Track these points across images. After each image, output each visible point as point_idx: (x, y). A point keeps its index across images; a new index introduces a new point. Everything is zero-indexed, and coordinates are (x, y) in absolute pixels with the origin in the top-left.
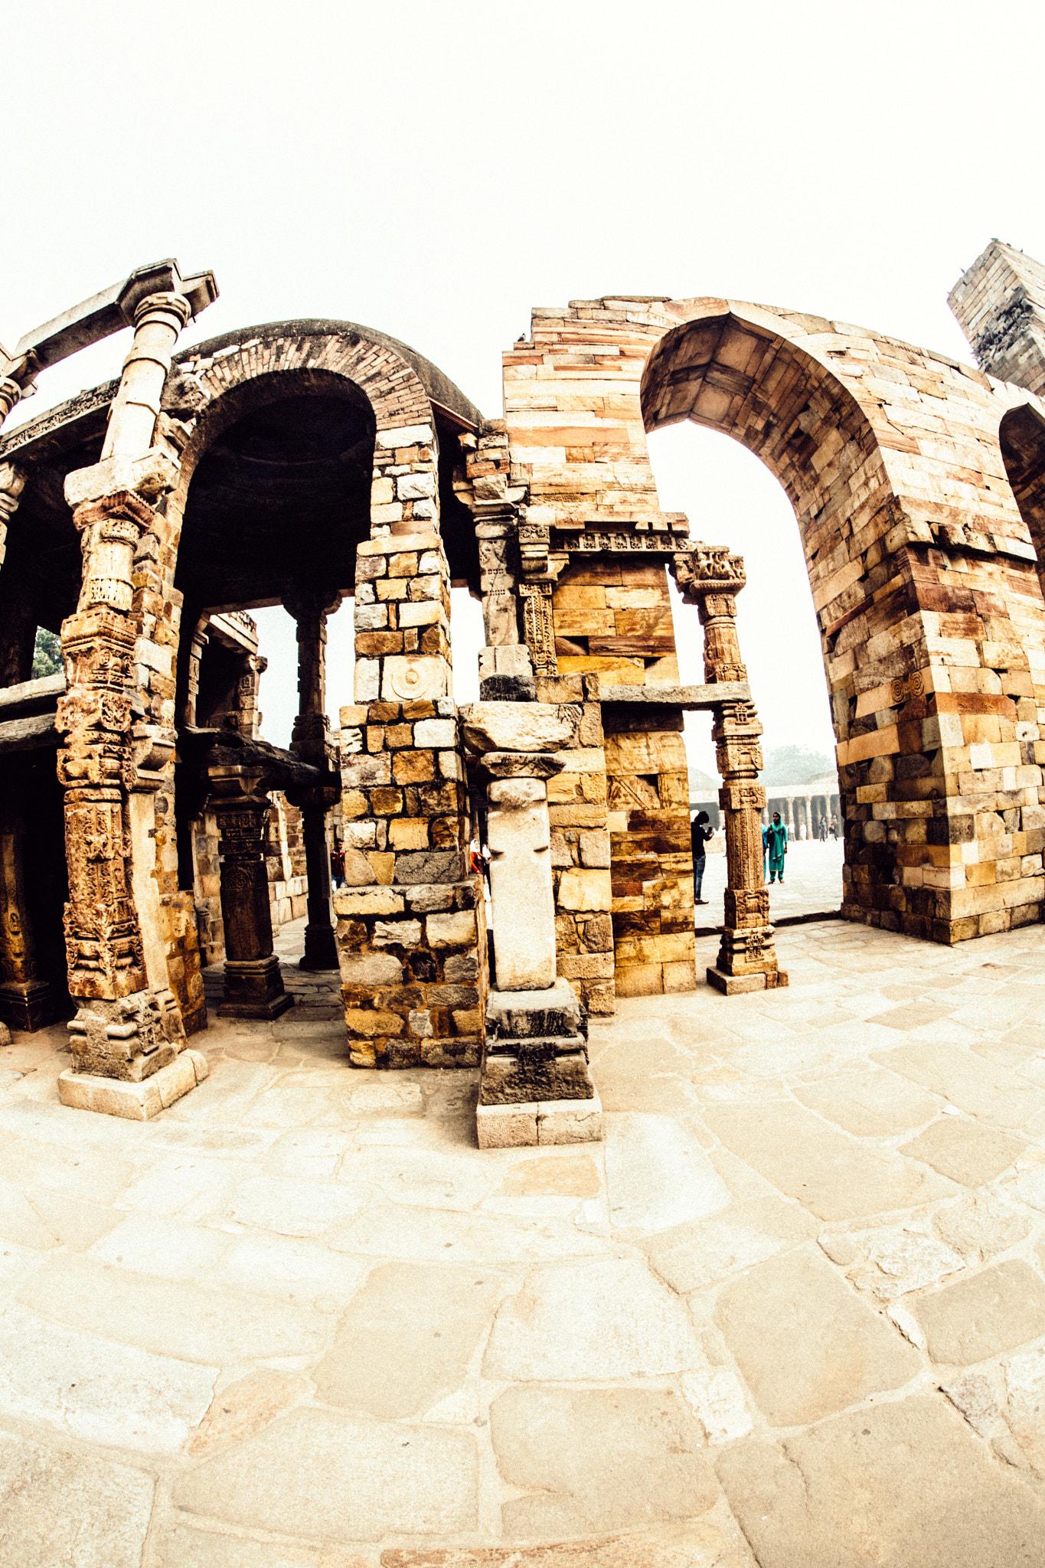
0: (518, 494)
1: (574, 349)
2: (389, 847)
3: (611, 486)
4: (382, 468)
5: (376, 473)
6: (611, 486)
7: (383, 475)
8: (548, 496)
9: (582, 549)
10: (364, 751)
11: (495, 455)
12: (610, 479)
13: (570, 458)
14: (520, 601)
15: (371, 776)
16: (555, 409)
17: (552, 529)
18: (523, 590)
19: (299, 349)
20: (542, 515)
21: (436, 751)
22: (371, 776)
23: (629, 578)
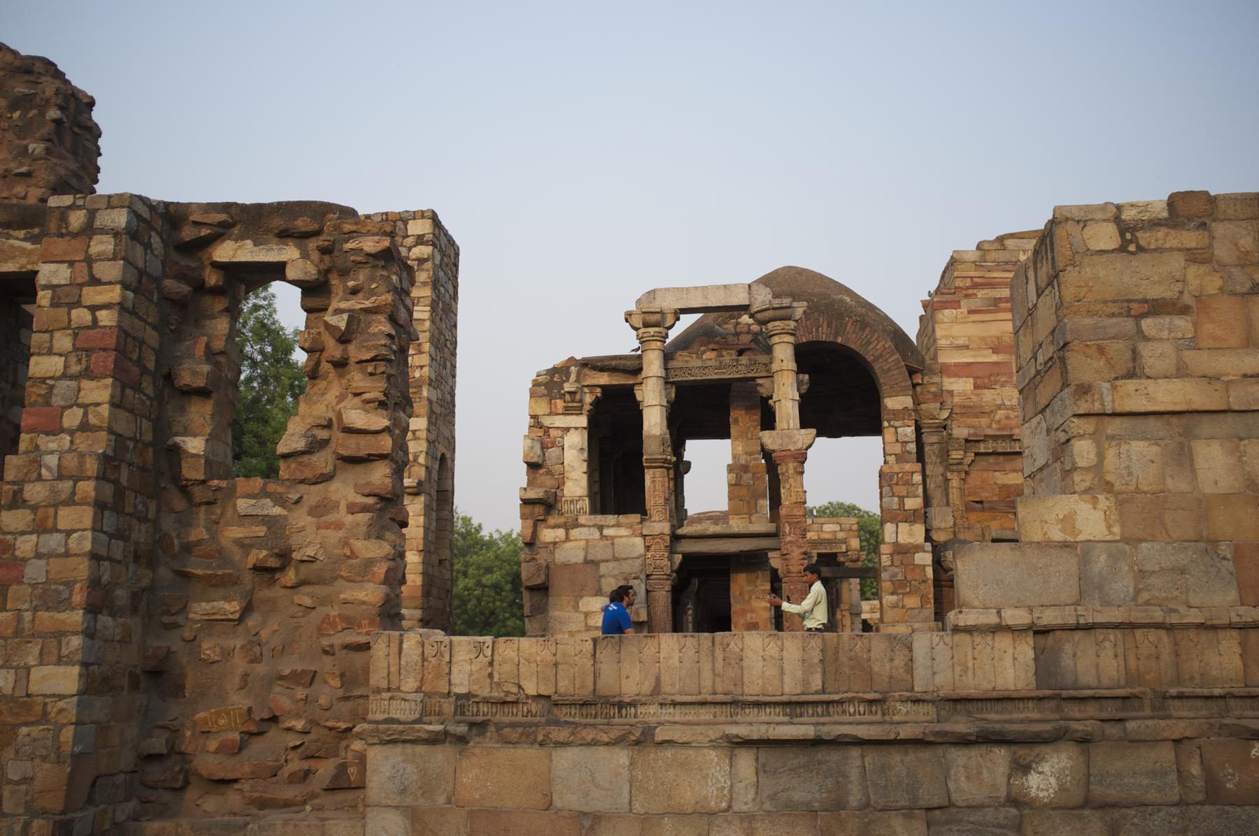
0: (945, 414)
1: (981, 293)
2: (903, 607)
3: (999, 407)
4: (889, 421)
5: (886, 424)
6: (999, 407)
7: (890, 426)
8: (962, 414)
9: (982, 450)
10: (892, 565)
11: (933, 389)
12: (999, 402)
13: (976, 387)
14: (947, 481)
15: (896, 575)
16: (967, 347)
17: (967, 441)
18: (949, 475)
19: (829, 326)
20: (960, 432)
21: (924, 566)
22: (896, 575)
23: (1008, 466)
